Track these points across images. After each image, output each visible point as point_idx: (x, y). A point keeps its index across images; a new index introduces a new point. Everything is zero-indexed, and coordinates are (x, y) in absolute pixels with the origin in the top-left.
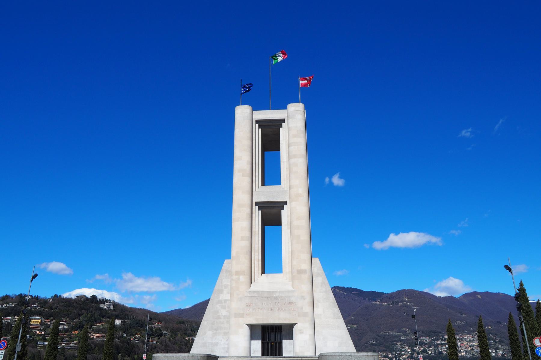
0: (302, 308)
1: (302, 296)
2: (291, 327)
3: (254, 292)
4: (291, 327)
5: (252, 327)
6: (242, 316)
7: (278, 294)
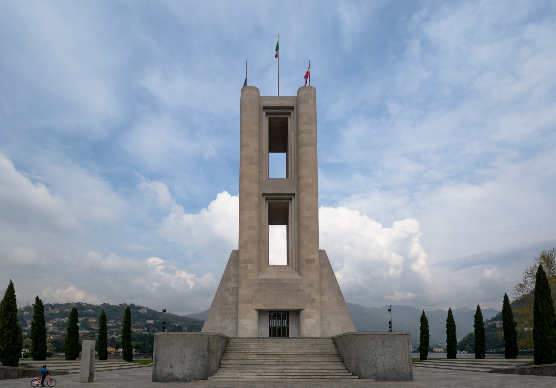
0: (309, 295)
1: (311, 284)
2: (297, 312)
3: (262, 279)
4: (297, 312)
5: (260, 312)
6: (250, 301)
7: (286, 282)
